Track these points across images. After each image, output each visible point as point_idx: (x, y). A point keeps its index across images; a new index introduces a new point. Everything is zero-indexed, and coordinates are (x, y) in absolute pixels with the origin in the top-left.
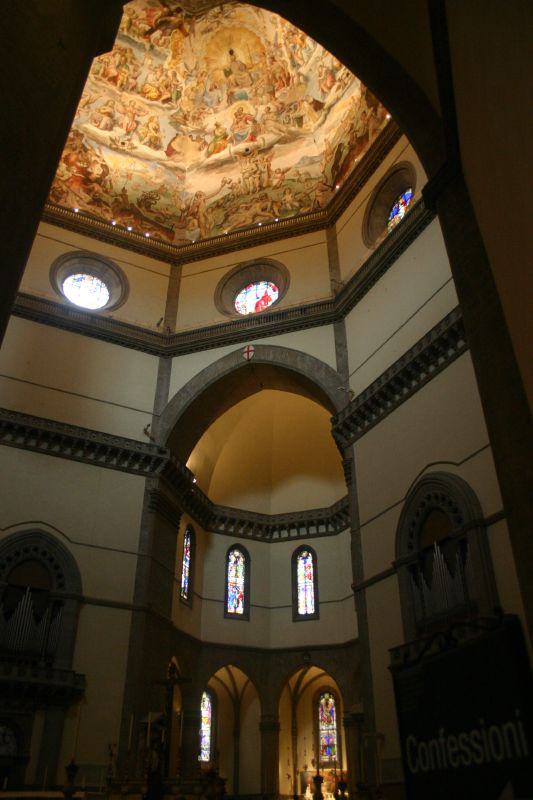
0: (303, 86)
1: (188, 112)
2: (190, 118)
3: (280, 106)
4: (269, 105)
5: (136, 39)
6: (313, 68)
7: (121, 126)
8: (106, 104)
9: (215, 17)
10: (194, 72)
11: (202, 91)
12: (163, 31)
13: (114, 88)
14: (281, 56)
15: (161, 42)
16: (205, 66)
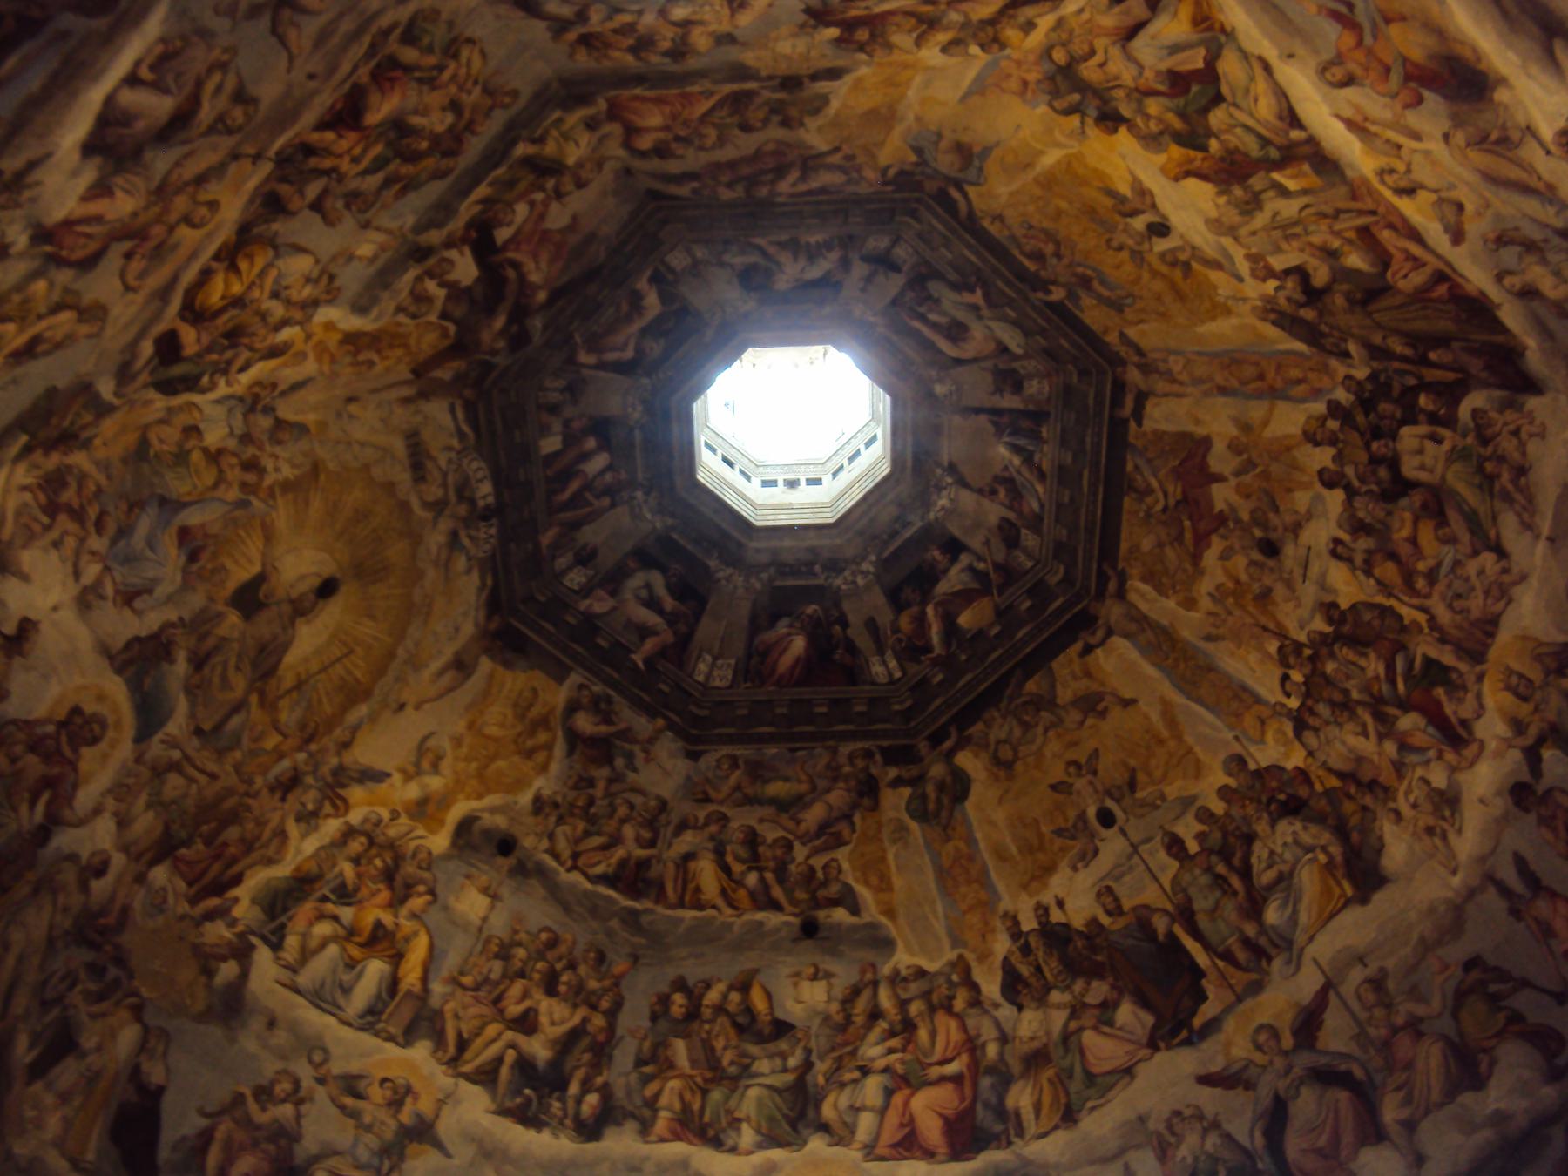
0: (200, 1006)
1: (86, 445)
2: (54, 460)
3: (111, 920)
4: (118, 860)
5: (482, 191)
6: (281, 1037)
7: (101, 189)
8: (241, 97)
9: (464, 491)
10: (265, 422)
11: (177, 485)
12: (469, 289)
13: (310, 117)
14: (298, 820)
15: (431, 286)
16: (288, 472)
